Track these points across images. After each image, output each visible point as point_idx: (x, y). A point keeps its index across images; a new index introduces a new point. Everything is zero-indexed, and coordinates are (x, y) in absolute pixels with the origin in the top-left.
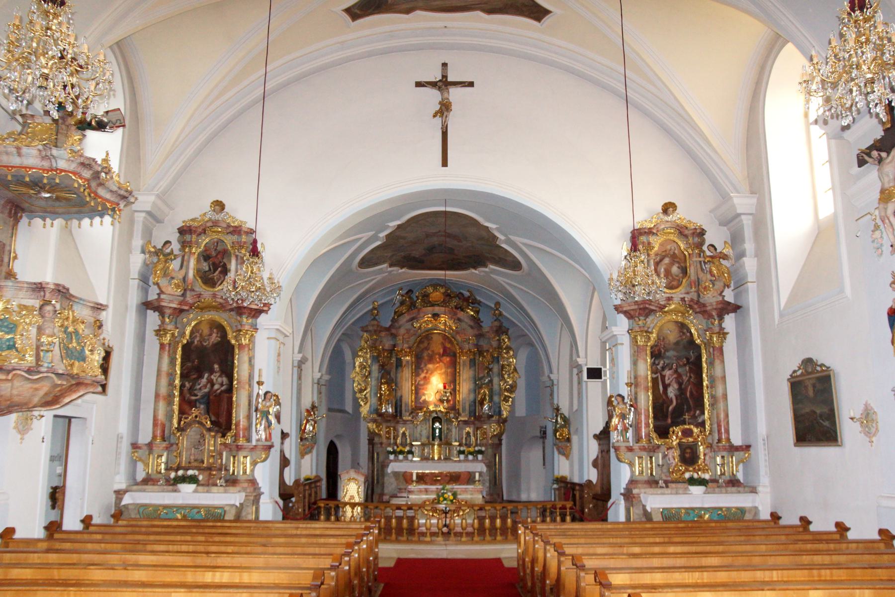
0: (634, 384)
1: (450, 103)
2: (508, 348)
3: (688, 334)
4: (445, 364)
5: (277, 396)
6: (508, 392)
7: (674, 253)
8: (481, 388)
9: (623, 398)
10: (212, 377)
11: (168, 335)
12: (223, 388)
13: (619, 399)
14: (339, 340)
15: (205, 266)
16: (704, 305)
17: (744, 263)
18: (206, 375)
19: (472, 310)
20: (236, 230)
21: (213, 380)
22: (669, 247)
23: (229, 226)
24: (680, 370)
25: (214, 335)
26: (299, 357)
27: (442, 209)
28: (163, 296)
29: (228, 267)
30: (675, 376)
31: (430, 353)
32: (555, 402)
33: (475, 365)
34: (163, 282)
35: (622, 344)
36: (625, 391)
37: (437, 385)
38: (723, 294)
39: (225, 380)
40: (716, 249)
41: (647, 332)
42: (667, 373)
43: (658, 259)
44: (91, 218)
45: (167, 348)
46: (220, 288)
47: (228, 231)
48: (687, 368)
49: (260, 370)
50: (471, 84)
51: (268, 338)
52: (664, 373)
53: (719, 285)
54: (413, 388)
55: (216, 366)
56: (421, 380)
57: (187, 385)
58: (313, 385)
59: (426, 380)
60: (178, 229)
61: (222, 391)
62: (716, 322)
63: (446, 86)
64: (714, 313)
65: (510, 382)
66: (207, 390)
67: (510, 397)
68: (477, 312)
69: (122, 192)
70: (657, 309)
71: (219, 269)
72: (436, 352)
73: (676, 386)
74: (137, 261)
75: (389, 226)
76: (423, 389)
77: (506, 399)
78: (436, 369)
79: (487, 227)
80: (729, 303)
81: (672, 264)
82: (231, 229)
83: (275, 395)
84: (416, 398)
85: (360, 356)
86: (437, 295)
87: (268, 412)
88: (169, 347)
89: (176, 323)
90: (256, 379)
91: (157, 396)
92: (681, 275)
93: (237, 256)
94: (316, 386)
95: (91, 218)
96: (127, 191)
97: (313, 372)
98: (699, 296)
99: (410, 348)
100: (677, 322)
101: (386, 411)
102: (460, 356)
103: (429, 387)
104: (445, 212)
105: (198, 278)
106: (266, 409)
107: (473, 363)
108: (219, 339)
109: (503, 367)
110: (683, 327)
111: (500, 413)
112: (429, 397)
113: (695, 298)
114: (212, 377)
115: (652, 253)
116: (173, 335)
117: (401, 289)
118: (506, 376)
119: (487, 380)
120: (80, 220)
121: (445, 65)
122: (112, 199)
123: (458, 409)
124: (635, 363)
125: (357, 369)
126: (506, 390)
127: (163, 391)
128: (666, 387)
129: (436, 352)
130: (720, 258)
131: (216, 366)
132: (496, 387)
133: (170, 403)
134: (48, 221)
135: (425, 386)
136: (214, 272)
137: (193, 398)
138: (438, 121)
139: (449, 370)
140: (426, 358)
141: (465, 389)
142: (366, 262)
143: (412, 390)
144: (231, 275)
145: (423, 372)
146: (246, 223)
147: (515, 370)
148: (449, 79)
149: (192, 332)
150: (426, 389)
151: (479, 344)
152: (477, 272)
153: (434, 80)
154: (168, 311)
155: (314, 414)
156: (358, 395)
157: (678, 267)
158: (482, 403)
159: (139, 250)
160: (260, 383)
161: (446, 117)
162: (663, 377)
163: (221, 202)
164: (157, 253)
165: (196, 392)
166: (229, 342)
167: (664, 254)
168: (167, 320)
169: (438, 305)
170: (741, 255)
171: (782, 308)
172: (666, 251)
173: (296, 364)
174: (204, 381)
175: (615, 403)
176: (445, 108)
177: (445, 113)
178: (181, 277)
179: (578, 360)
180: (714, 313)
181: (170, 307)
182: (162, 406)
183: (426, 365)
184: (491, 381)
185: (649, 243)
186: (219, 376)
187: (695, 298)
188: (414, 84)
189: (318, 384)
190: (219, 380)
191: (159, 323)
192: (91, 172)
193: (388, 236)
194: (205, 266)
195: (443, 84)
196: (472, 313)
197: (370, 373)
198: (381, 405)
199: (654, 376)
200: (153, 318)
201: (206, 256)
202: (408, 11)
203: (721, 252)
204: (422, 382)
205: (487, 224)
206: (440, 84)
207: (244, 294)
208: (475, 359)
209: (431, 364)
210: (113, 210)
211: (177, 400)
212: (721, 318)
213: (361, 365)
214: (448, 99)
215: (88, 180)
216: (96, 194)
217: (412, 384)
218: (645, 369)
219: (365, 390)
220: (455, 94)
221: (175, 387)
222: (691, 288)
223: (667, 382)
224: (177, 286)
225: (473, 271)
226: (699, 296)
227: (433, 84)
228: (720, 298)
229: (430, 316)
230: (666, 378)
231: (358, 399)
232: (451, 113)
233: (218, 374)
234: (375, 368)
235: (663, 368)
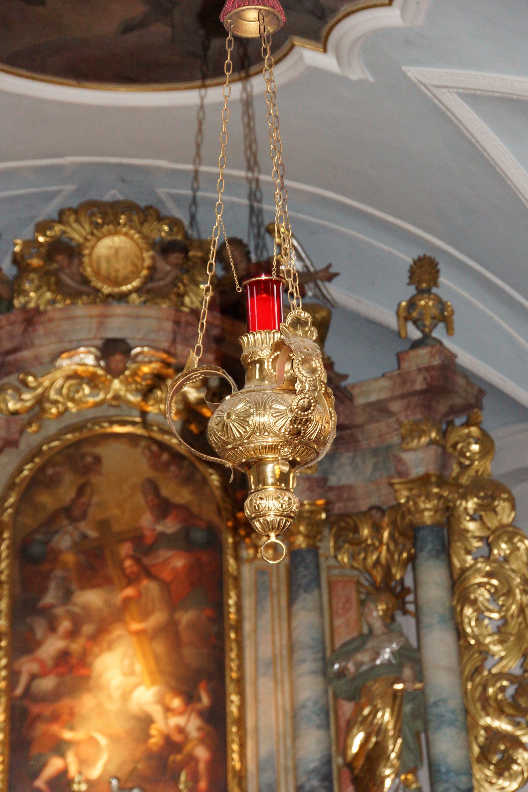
4: (165, 586)
31: (93, 534)
33: (319, 586)
37: (126, 696)
56: (44, 673)
72: (116, 528)
76: (55, 718)
112: (83, 762)
119: (386, 654)
129: (116, 528)
135: (66, 703)
140: (70, 558)
145: (52, 629)
151: (333, 481)
208: (314, 550)
209: (93, 586)
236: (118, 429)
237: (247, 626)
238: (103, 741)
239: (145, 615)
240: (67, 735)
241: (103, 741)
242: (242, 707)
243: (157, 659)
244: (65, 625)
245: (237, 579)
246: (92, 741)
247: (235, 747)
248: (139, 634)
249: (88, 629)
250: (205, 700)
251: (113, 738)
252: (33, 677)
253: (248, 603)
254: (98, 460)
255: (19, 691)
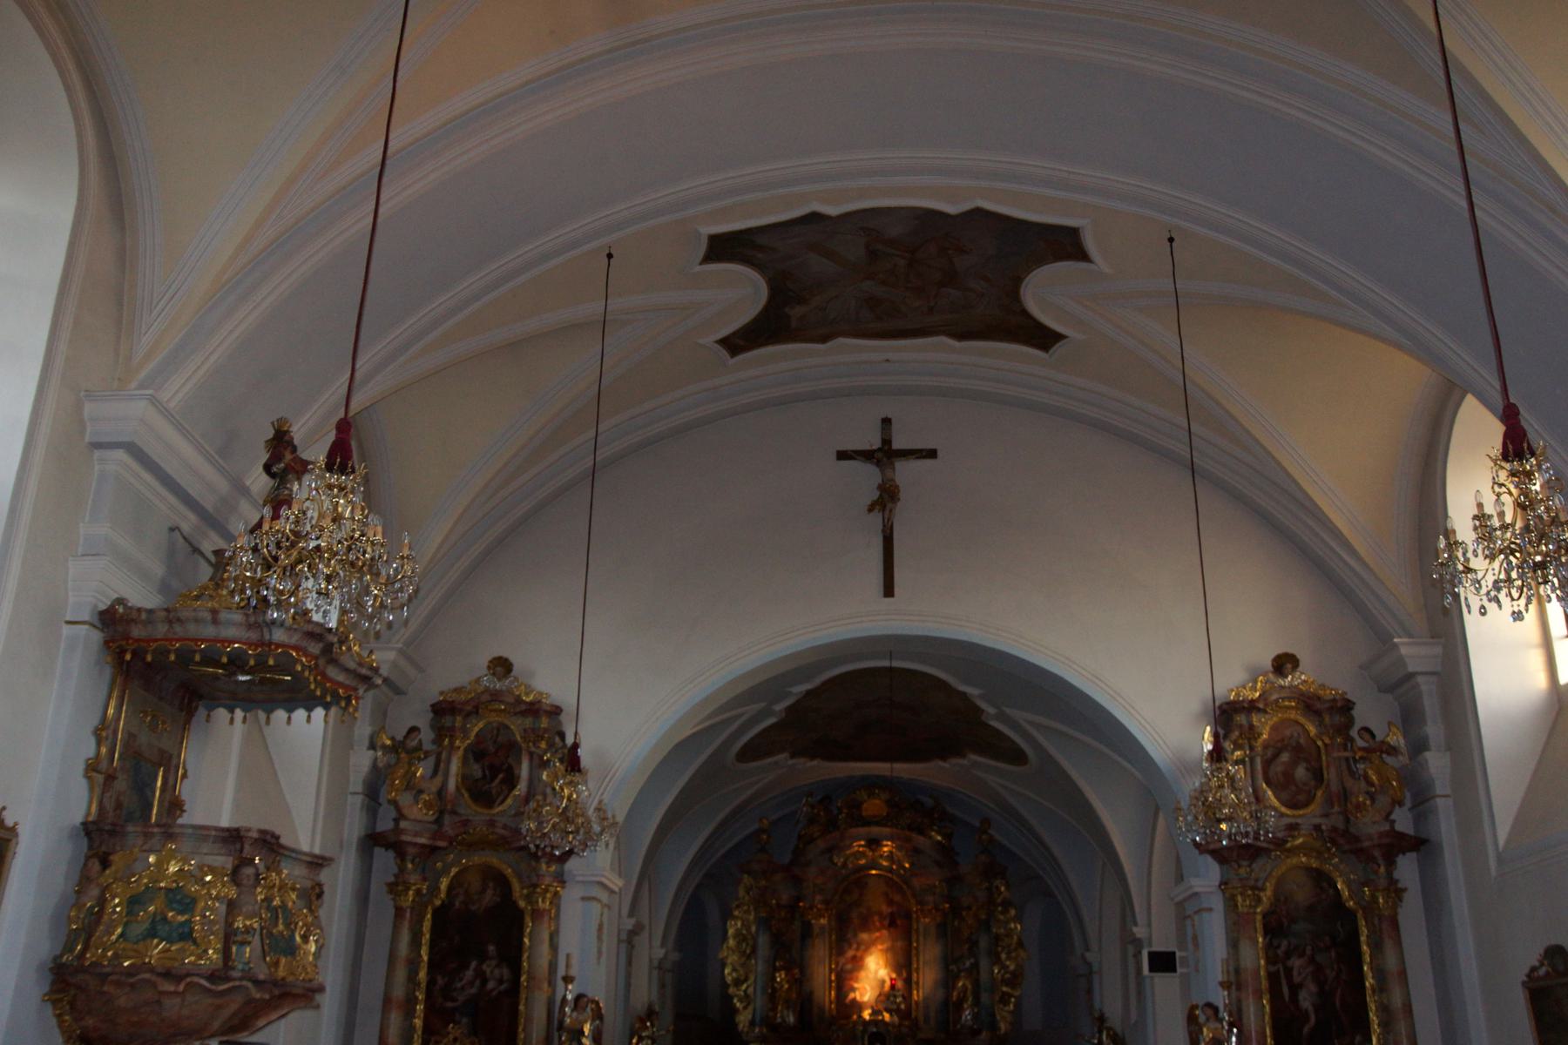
0: (1234, 982)
1: (897, 487)
2: (1007, 904)
3: (1331, 891)
5: (597, 1003)
6: (1007, 985)
7: (1298, 743)
8: (957, 978)
9: (1216, 1010)
10: (484, 967)
11: (411, 893)
12: (503, 987)
13: (1210, 1012)
14: (698, 886)
15: (476, 770)
16: (1357, 839)
17: (1426, 761)
18: (474, 964)
19: (939, 833)
20: (534, 709)
21: (484, 972)
22: (1288, 733)
23: (519, 700)
24: (1319, 958)
25: (490, 892)
26: (629, 924)
27: (885, 663)
28: (403, 824)
29: (516, 772)
30: (1310, 969)
32: (1097, 1005)
34: (405, 800)
35: (1210, 910)
36: (1220, 998)
37: (876, 972)
38: (1393, 817)
39: (506, 972)
40: (1373, 736)
41: (1253, 888)
42: (1296, 963)
43: (1270, 753)
44: (310, 709)
45: (408, 915)
46: (501, 808)
47: (518, 710)
48: (1333, 954)
49: (568, 956)
50: (932, 454)
51: (583, 899)
52: (1290, 963)
53: (1383, 801)
54: (833, 978)
55: (491, 948)
57: (440, 981)
58: (650, 973)
59: (858, 963)
60: (433, 706)
61: (500, 993)
62: (1382, 869)
63: (889, 458)
64: (1377, 853)
65: (1012, 967)
66: (473, 991)
67: (1010, 996)
68: (948, 837)
69: (364, 671)
70: (1271, 847)
71: (501, 776)
73: (1313, 988)
74: (362, 761)
75: (790, 692)
76: (851, 979)
77: (1005, 999)
78: (873, 943)
79: (964, 694)
80: (1402, 836)
81: (1294, 763)
82: (523, 707)
83: (593, 1001)
84: (838, 996)
85: (736, 918)
86: (874, 806)
87: (582, 1033)
88: (411, 913)
89: (423, 870)
90: (561, 972)
91: (387, 1001)
92: (1313, 783)
93: (531, 754)
94: (655, 973)
95: (310, 709)
96: (371, 668)
97: (651, 947)
98: (1347, 821)
99: (826, 902)
100: (1308, 869)
101: (784, 1021)
102: (918, 918)
103: (863, 974)
104: (891, 669)
105: (463, 791)
106: (578, 1027)
107: (943, 931)
108: (498, 899)
109: (997, 938)
110: (1321, 879)
111: (993, 1026)
112: (862, 995)
113: (1341, 826)
114: (484, 967)
115: (1259, 744)
116: (418, 892)
117: (811, 794)
118: (1003, 956)
119: (968, 964)
120: (290, 710)
121: (886, 422)
122: (347, 682)
123: (916, 1018)
124: (1233, 944)
125: (731, 942)
126: (1005, 982)
127: (399, 992)
128: (1295, 989)
130: (1382, 752)
131: (491, 948)
132: (984, 977)
133: (409, 1013)
134: (239, 713)
135: (855, 974)
136: (492, 780)
137: (449, 1005)
138: (876, 519)
139: (899, 944)
141: (927, 979)
142: (752, 752)
143: (831, 981)
144: (521, 788)
145: (850, 946)
146: (548, 696)
147: (1020, 944)
148: (896, 445)
149: (450, 888)
150: (857, 980)
152: (946, 765)
153: (867, 447)
154: (411, 850)
155: (652, 1025)
156: (731, 990)
157: (1307, 769)
158: (959, 1006)
159: (366, 743)
160: (568, 979)
161: (891, 511)
162: (1289, 971)
163: (506, 660)
164: (396, 748)
165: (455, 994)
166: (515, 903)
167: (1279, 745)
168: (410, 866)
169: (878, 824)
170: (1419, 746)
171: (1501, 842)
172: (1283, 740)
173: (624, 936)
174: (470, 973)
175: (1202, 1019)
176: (887, 497)
177: (889, 505)
178: (434, 789)
179: (1135, 929)
180: (1377, 853)
181: (415, 844)
182: (395, 1018)
183: (855, 935)
184: (976, 966)
185: (1251, 727)
186: (497, 966)
187: (1341, 826)
188: (834, 456)
189: (660, 968)
190: (495, 972)
191: (396, 870)
192: (321, 645)
193: (789, 709)
194: (476, 770)
195: (885, 455)
196: (939, 838)
197: (754, 950)
198: (774, 1009)
199: (1273, 969)
200: (384, 860)
201: (477, 753)
202: (824, 339)
203: (1383, 742)
204: (849, 966)
205: (963, 688)
206: (879, 455)
207: (556, 838)
210: (348, 700)
211: (420, 1007)
212: (1391, 863)
213: (738, 934)
214: (893, 480)
215: (316, 658)
216: (324, 675)
217: (831, 971)
218: (1253, 956)
219: (746, 980)
220: (905, 472)
221: (419, 984)
222: (1333, 807)
223: (1297, 979)
224: (428, 805)
225: (941, 763)
226: (1347, 821)
227: (867, 456)
228: (1387, 827)
229: (863, 843)
230: (1295, 973)
231: (730, 998)
232: (899, 504)
233: (494, 963)
234: (763, 941)
235: (1288, 955)
236: (874, 872)
237: (921, 948)
238: (868, 988)
239: (882, 944)
240: (856, 985)
241: (868, 988)
242: (918, 978)
243: (887, 959)
244: (855, 946)
245: (917, 930)
246: (865, 989)
247: (915, 992)
248: (881, 950)
249: (863, 947)
250: (905, 975)
251: (872, 988)
252: (844, 964)
253: (921, 939)
254: (866, 884)
255: (839, 969)
